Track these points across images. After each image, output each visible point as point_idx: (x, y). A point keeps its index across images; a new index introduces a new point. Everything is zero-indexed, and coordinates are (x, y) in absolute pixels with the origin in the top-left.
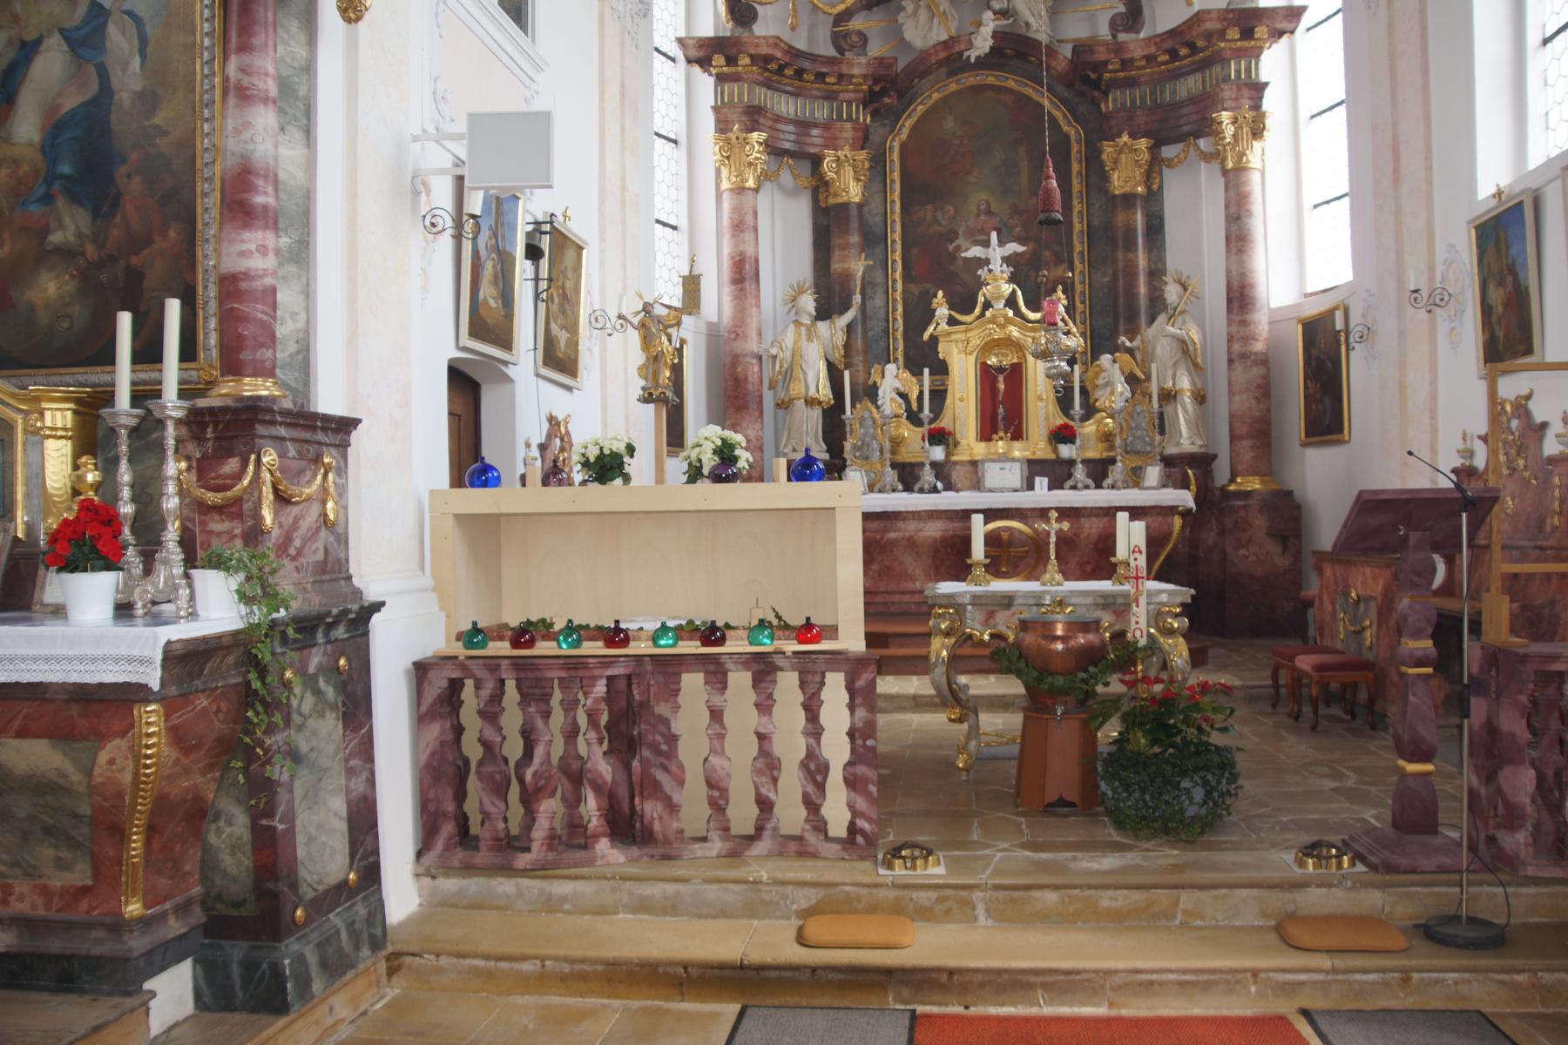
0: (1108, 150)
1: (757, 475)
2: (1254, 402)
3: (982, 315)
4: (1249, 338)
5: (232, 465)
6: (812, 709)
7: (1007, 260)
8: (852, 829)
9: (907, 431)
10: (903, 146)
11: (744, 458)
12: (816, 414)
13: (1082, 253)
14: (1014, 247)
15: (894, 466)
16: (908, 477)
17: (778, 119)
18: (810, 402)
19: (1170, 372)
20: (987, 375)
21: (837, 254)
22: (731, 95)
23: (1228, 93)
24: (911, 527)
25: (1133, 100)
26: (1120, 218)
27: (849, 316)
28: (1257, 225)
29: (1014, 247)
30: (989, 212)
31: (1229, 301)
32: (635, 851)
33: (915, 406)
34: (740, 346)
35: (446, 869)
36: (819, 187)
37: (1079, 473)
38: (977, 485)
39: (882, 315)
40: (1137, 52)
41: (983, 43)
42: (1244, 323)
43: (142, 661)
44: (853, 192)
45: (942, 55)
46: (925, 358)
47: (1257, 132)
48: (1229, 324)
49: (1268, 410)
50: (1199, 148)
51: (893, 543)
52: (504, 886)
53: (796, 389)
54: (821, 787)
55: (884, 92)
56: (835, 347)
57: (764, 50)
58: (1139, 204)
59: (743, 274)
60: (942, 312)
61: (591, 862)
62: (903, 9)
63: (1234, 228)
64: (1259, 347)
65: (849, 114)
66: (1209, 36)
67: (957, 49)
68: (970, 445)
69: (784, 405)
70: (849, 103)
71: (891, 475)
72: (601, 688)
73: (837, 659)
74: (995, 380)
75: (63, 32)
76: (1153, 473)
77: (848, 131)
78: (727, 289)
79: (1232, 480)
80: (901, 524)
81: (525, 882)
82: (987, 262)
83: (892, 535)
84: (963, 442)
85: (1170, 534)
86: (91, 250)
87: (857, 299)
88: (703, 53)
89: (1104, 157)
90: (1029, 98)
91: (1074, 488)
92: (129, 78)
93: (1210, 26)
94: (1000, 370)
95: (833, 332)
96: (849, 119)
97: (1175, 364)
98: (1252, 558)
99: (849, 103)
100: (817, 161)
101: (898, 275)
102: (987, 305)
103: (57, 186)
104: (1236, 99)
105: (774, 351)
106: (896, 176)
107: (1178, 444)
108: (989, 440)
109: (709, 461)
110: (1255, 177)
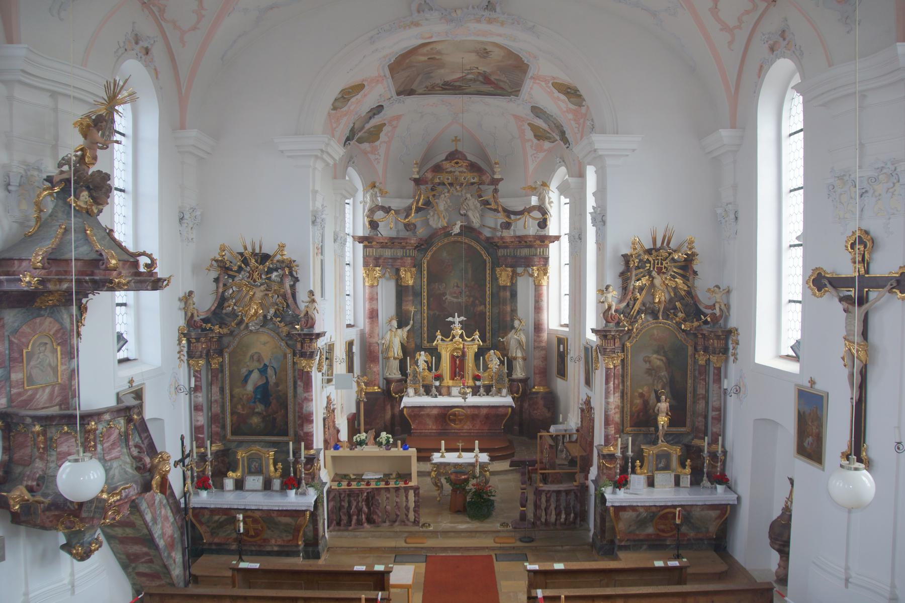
0: (498, 270)
1: (395, 445)
2: (541, 363)
3: (451, 340)
4: (541, 341)
5: (309, 466)
6: (407, 498)
7: (459, 322)
8: (415, 520)
9: (427, 373)
10: (428, 262)
11: (391, 440)
12: (397, 362)
13: (489, 302)
14: (462, 318)
15: (423, 386)
16: (428, 391)
17: (385, 259)
18: (395, 358)
19: (515, 351)
20: (453, 358)
21: (404, 304)
22: (369, 252)
23: (536, 259)
24: (428, 410)
25: (507, 253)
26: (502, 294)
27: (408, 327)
28: (544, 304)
29: (462, 318)
30: (458, 286)
31: (535, 328)
32: (372, 525)
33: (430, 365)
34: (374, 340)
35: (334, 530)
36: (398, 279)
37: (482, 390)
38: (449, 394)
39: (420, 322)
40: (508, 240)
41: (457, 230)
42: (539, 337)
43: (309, 506)
44: (411, 283)
45: (443, 232)
46: (434, 352)
47: (545, 272)
48: (535, 335)
49: (546, 365)
50: (529, 273)
51: (424, 415)
52: (346, 533)
53: (391, 354)
54: (408, 512)
55: (422, 245)
56: (404, 339)
57: (382, 241)
58: (508, 289)
59: (373, 315)
60: (439, 337)
61: (363, 528)
62: (429, 214)
63: (537, 304)
64: (544, 344)
65: (409, 254)
66: (530, 241)
67: (448, 230)
68: (448, 381)
69: (387, 358)
70: (410, 250)
71: (422, 390)
72: (365, 494)
73: (411, 487)
74: (456, 360)
75: (258, 369)
76: (504, 391)
77: (409, 261)
78: (367, 320)
79: (534, 387)
80: (425, 409)
81: (350, 533)
82: (454, 323)
83: (422, 413)
84: (445, 379)
85: (508, 413)
86: (264, 413)
87: (411, 322)
88: (361, 240)
89: (497, 272)
90: (472, 246)
91: (480, 395)
92: (273, 380)
93: (530, 239)
94: (458, 357)
95: (403, 333)
96: (410, 256)
97: (517, 348)
98: (538, 414)
99: (410, 250)
100: (398, 270)
101: (425, 308)
102: (454, 337)
103: (256, 400)
104: (539, 262)
105: (383, 342)
106: (425, 272)
107: (516, 375)
108: (453, 379)
109: (384, 442)
110: (545, 288)
